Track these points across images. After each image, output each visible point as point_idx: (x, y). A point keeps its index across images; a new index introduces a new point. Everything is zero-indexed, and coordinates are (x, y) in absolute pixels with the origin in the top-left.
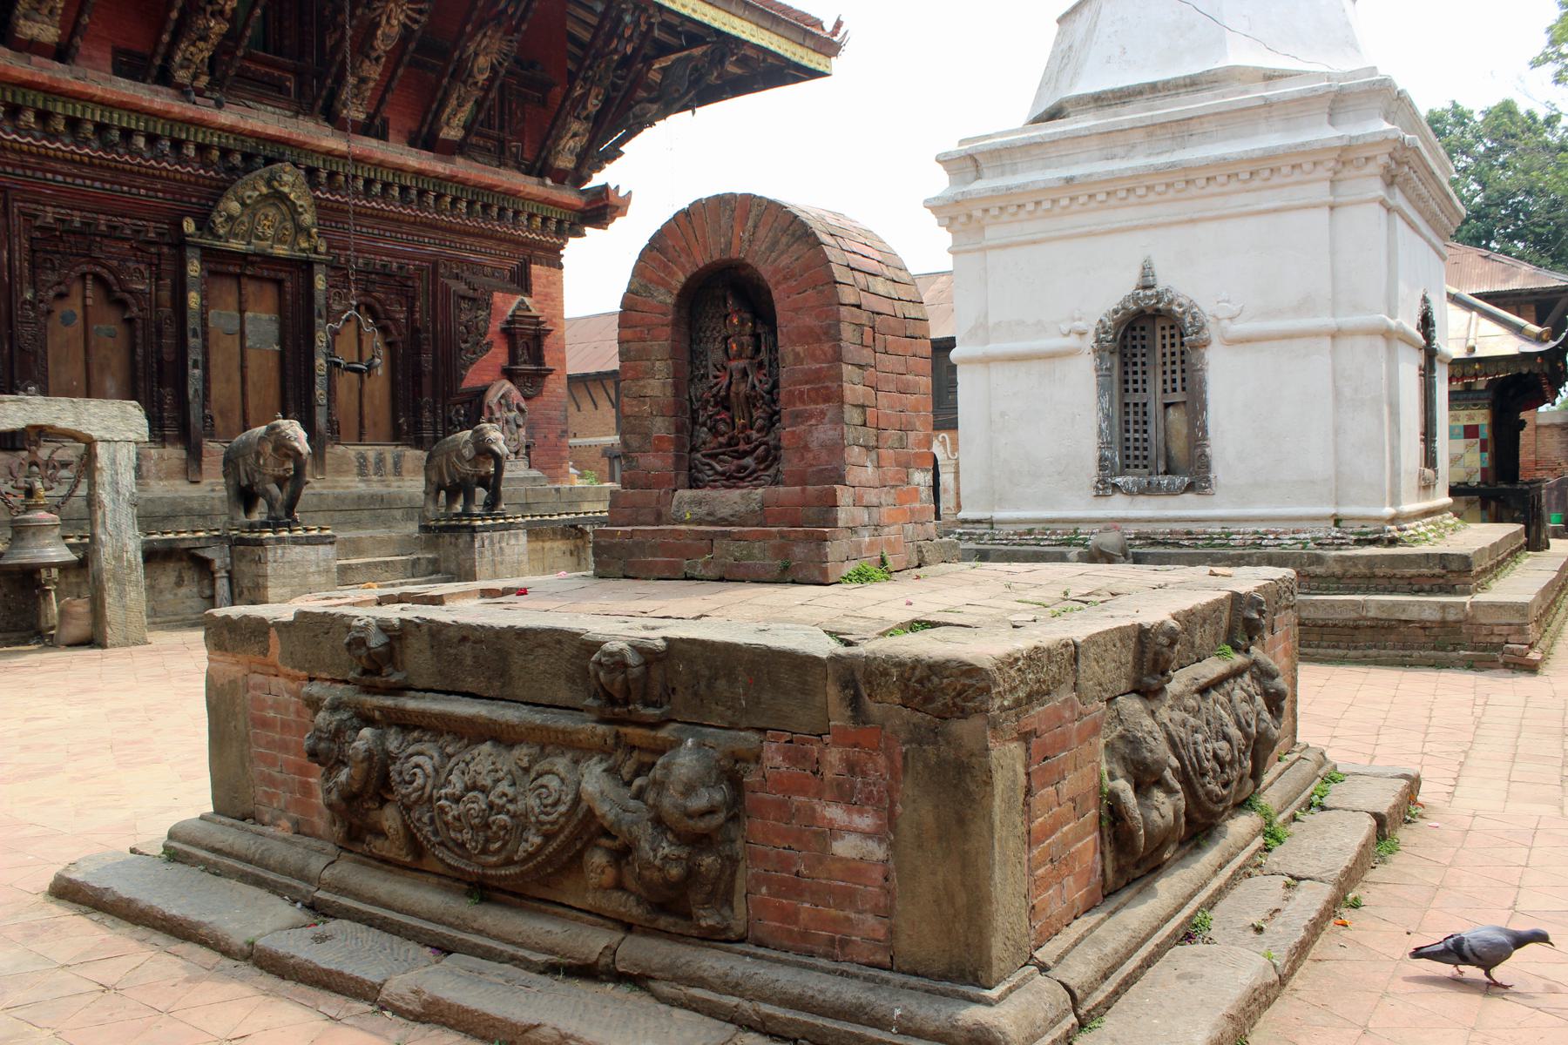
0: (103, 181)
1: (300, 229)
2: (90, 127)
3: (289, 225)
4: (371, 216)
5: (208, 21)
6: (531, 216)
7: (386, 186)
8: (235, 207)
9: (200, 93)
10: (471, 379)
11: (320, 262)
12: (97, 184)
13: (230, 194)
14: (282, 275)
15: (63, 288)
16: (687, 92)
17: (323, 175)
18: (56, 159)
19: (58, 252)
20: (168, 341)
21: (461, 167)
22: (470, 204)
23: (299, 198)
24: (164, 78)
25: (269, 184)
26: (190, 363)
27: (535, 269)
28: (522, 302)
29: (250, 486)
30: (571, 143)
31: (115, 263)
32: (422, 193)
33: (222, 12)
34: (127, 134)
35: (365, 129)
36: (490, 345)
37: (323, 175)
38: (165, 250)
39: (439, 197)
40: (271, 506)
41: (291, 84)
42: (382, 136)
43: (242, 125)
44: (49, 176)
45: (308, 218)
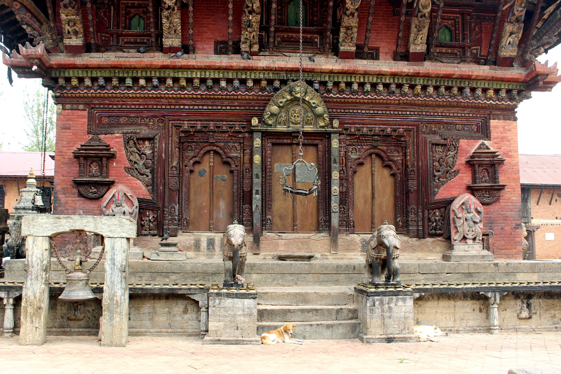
0: (208, 105)
3: (310, 114)
4: (368, 103)
5: (248, 17)
6: (485, 90)
7: (374, 85)
9: (256, 54)
10: (442, 194)
11: (335, 133)
12: (205, 107)
13: (271, 102)
14: (317, 142)
15: (197, 159)
18: (185, 98)
19: (194, 142)
21: (428, 67)
23: (312, 99)
24: (237, 51)
25: (291, 95)
26: (254, 192)
27: (493, 123)
28: (483, 144)
30: (510, 39)
31: (223, 144)
32: (400, 86)
34: (216, 81)
35: (359, 54)
36: (457, 172)
37: (330, 85)
38: (247, 135)
42: (374, 55)
43: (272, 65)
44: (182, 107)
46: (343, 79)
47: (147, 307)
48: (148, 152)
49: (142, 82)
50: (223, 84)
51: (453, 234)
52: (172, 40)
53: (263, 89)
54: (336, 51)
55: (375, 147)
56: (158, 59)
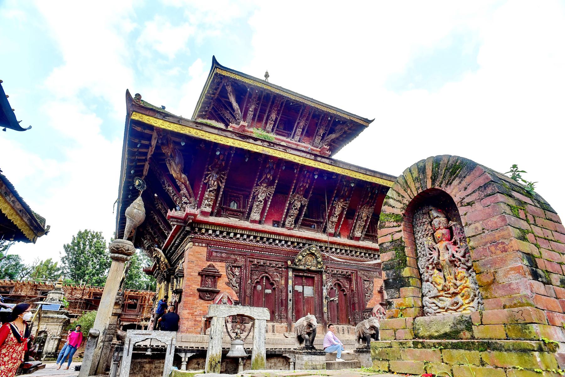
1: (319, 263)
8: (300, 257)
15: (258, 280)
17: (324, 248)
20: (284, 294)
22: (365, 254)
24: (283, 226)
29: (301, 335)
34: (274, 240)
40: (306, 342)
47: (273, 360)
48: (237, 274)
49: (238, 236)
50: (277, 242)
52: (256, 216)
54: (324, 231)
55: (338, 280)
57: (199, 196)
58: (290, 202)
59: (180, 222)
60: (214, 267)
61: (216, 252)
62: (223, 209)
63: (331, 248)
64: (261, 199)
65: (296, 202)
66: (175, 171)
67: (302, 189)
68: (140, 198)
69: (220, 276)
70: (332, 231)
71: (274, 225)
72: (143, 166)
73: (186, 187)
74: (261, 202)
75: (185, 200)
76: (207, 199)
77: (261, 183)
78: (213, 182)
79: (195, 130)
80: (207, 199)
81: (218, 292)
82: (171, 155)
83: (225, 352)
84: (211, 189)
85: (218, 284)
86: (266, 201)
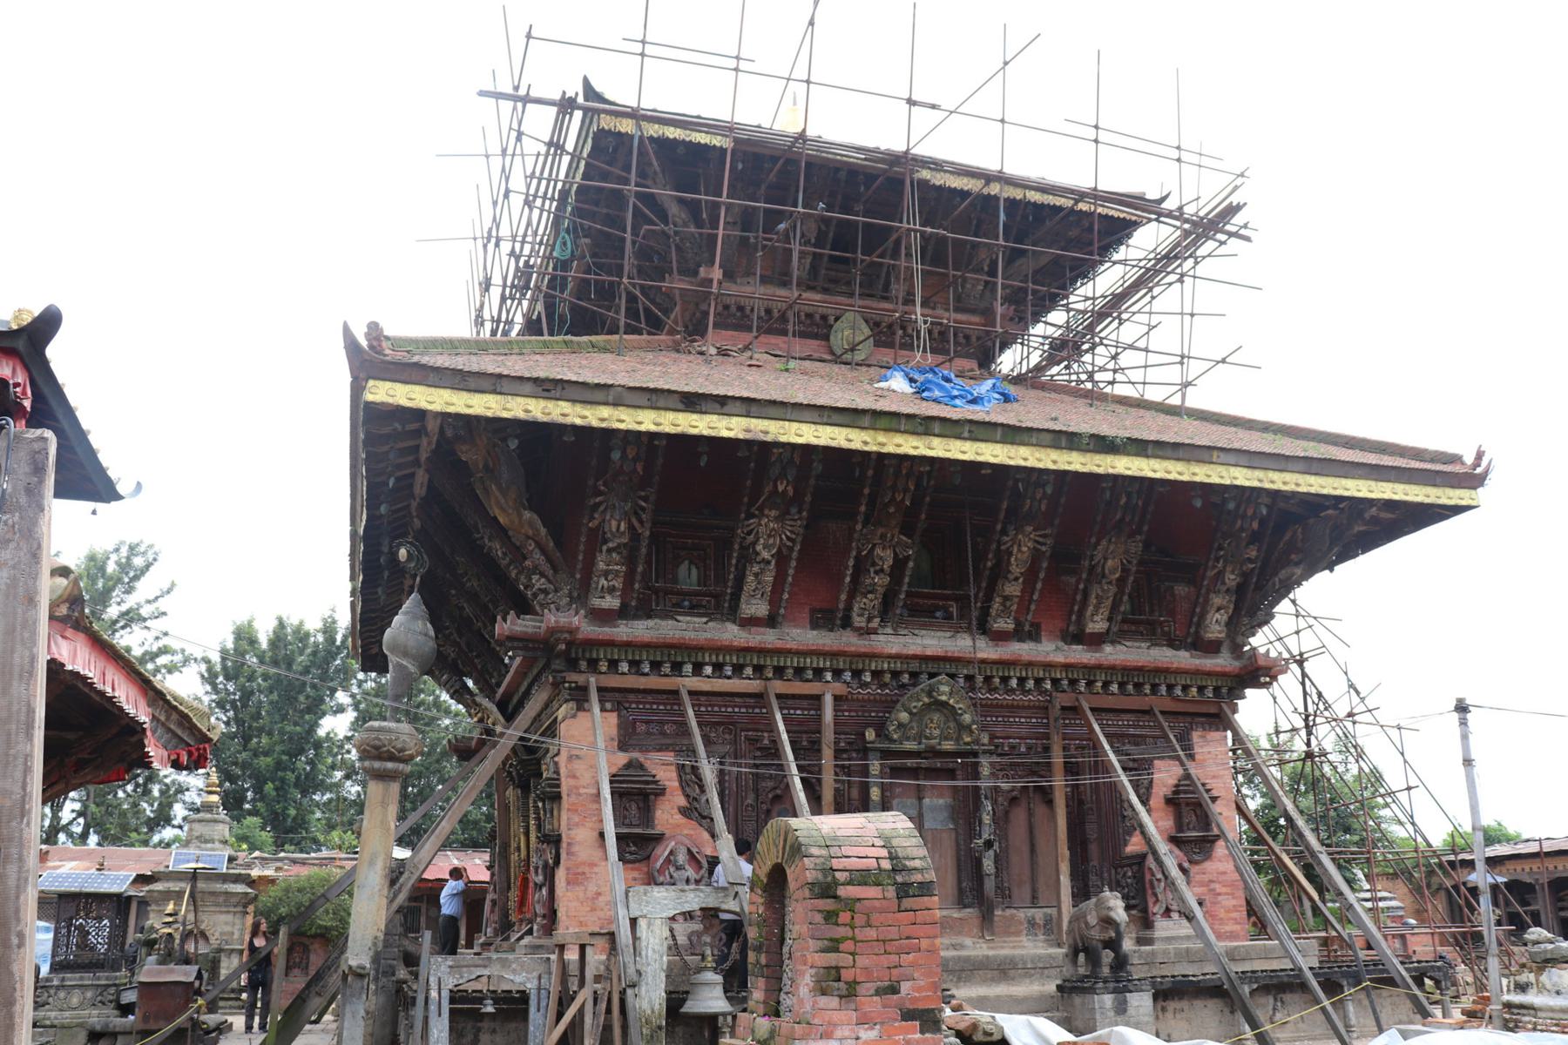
1: (963, 728)
2: (791, 671)
3: (952, 725)
4: (1029, 707)
13: (899, 706)
15: (779, 792)
16: (1330, 549)
17: (980, 679)
21: (1113, 654)
22: (1122, 685)
24: (846, 623)
25: (929, 695)
30: (1218, 616)
32: (1073, 682)
33: (882, 570)
35: (1019, 634)
37: (980, 679)
39: (1090, 684)
41: (954, 610)
42: (1034, 635)
45: (967, 718)
46: (997, 674)
51: (1151, 904)
52: (756, 607)
53: (883, 686)
54: (983, 628)
56: (731, 633)
57: (579, 566)
58: (859, 553)
59: (534, 649)
60: (641, 767)
61: (647, 722)
62: (656, 591)
63: (1005, 680)
64: (766, 555)
65: (878, 551)
66: (503, 510)
67: (892, 510)
68: (412, 602)
69: (662, 792)
70: (1004, 624)
71: (815, 625)
72: (413, 475)
73: (538, 544)
74: (768, 562)
75: (538, 582)
76: (606, 574)
77: (761, 509)
78: (616, 526)
79: (542, 403)
80: (606, 574)
81: (659, 838)
82: (486, 466)
83: (675, 1001)
84: (611, 545)
85: (658, 813)
86: (782, 558)
